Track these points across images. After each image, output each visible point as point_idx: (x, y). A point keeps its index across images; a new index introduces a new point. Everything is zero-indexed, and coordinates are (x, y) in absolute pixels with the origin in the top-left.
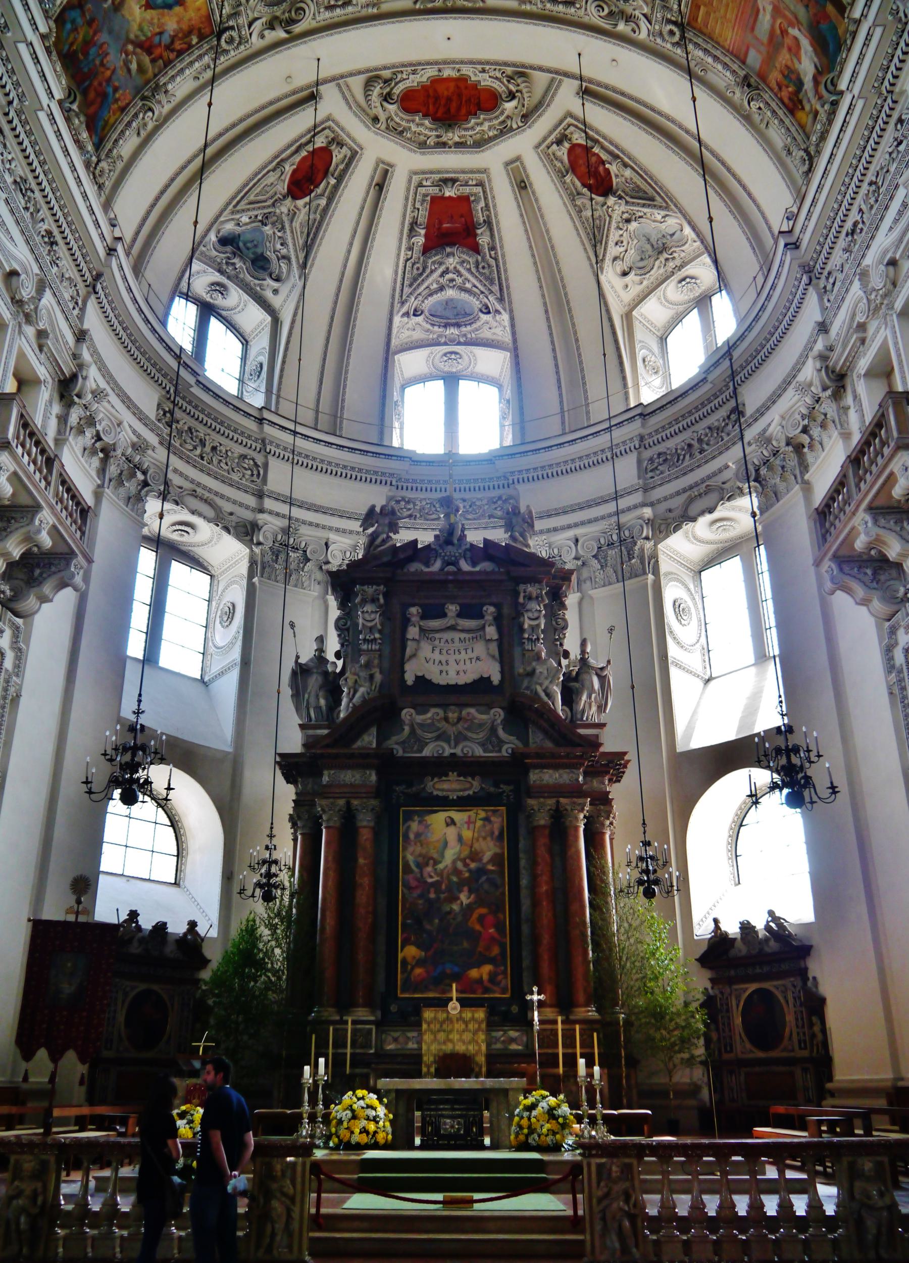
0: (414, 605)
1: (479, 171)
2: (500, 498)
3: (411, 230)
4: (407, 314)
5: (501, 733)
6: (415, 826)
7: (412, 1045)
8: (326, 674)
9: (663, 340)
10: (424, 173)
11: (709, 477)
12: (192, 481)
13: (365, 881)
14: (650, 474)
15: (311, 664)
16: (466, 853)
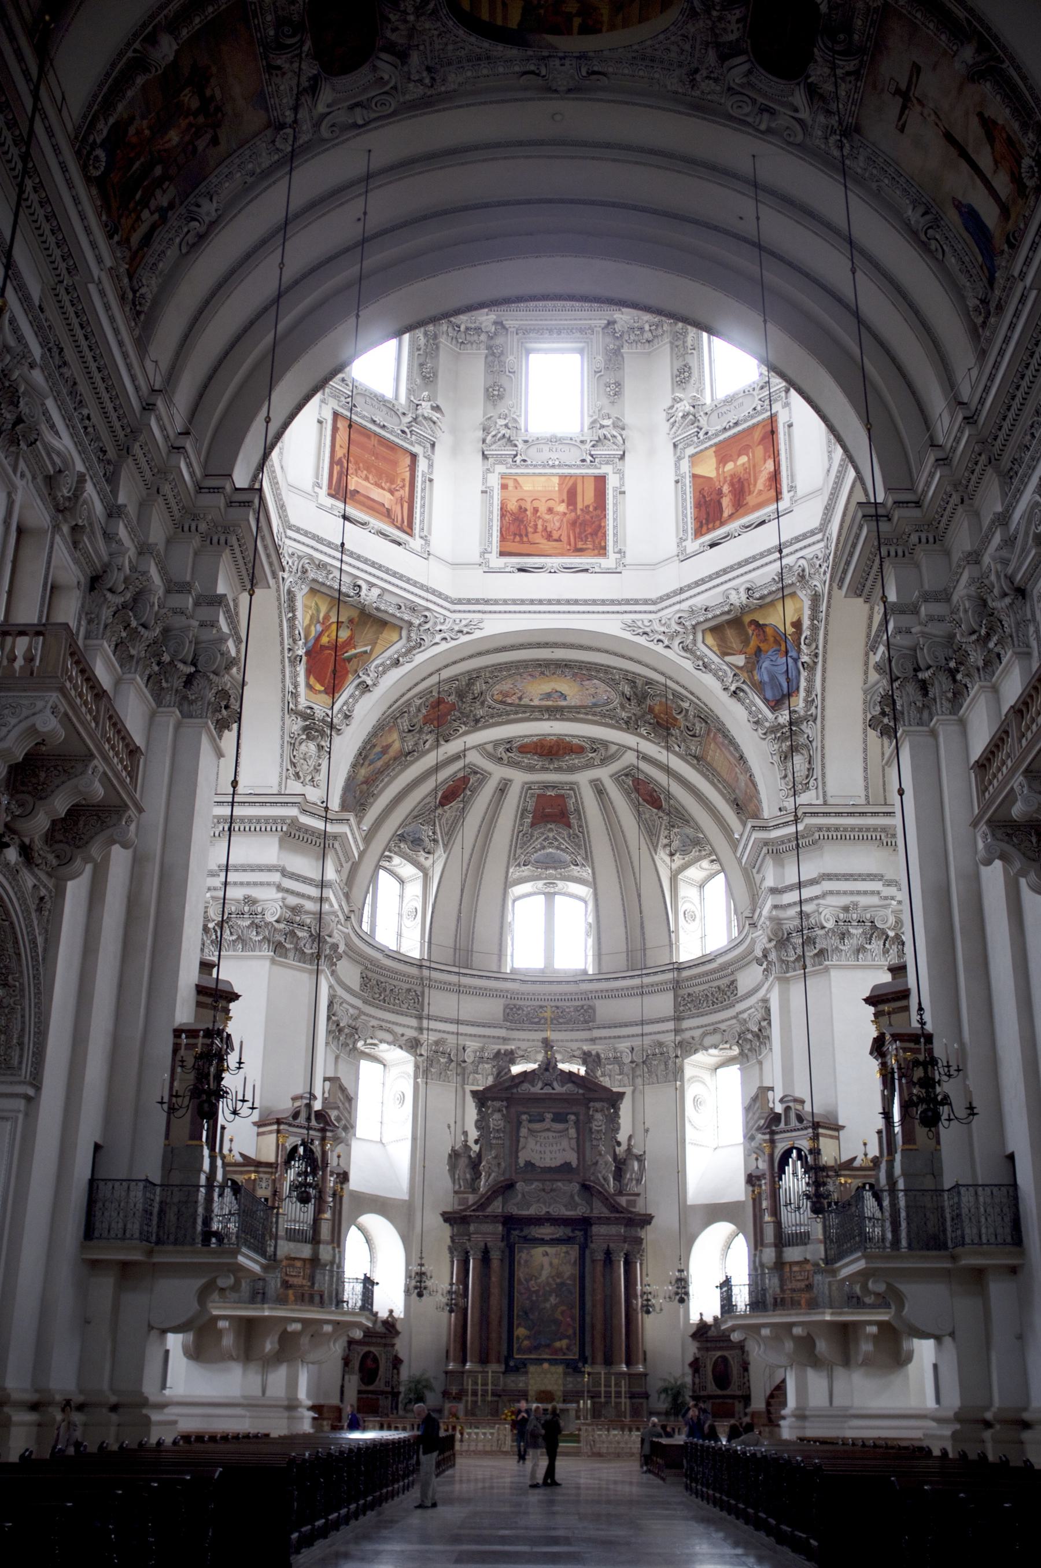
0: (525, 1113)
1: (571, 783)
2: (582, 1007)
3: (522, 814)
4: (519, 865)
5: (576, 1198)
6: (524, 1255)
7: (521, 1385)
8: (470, 1156)
9: (701, 886)
10: (533, 783)
11: (716, 1023)
12: (380, 1019)
13: (495, 1291)
14: (682, 1008)
15: (461, 1151)
16: (554, 1274)
